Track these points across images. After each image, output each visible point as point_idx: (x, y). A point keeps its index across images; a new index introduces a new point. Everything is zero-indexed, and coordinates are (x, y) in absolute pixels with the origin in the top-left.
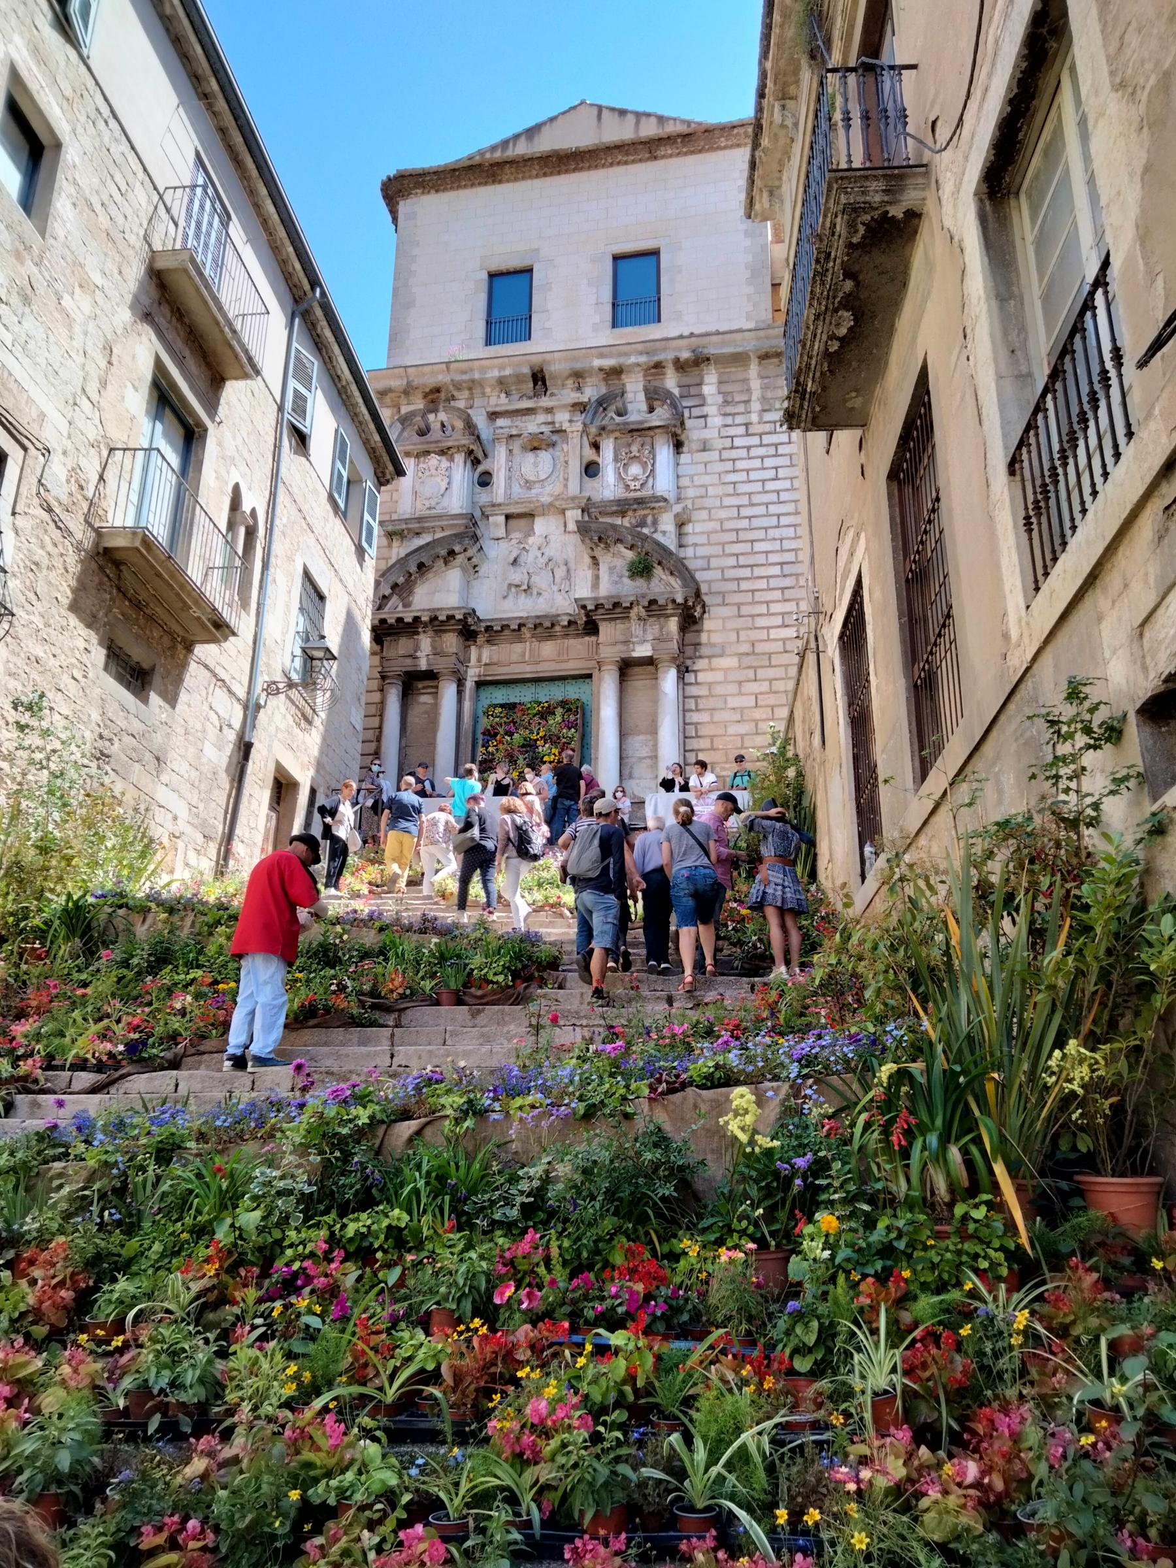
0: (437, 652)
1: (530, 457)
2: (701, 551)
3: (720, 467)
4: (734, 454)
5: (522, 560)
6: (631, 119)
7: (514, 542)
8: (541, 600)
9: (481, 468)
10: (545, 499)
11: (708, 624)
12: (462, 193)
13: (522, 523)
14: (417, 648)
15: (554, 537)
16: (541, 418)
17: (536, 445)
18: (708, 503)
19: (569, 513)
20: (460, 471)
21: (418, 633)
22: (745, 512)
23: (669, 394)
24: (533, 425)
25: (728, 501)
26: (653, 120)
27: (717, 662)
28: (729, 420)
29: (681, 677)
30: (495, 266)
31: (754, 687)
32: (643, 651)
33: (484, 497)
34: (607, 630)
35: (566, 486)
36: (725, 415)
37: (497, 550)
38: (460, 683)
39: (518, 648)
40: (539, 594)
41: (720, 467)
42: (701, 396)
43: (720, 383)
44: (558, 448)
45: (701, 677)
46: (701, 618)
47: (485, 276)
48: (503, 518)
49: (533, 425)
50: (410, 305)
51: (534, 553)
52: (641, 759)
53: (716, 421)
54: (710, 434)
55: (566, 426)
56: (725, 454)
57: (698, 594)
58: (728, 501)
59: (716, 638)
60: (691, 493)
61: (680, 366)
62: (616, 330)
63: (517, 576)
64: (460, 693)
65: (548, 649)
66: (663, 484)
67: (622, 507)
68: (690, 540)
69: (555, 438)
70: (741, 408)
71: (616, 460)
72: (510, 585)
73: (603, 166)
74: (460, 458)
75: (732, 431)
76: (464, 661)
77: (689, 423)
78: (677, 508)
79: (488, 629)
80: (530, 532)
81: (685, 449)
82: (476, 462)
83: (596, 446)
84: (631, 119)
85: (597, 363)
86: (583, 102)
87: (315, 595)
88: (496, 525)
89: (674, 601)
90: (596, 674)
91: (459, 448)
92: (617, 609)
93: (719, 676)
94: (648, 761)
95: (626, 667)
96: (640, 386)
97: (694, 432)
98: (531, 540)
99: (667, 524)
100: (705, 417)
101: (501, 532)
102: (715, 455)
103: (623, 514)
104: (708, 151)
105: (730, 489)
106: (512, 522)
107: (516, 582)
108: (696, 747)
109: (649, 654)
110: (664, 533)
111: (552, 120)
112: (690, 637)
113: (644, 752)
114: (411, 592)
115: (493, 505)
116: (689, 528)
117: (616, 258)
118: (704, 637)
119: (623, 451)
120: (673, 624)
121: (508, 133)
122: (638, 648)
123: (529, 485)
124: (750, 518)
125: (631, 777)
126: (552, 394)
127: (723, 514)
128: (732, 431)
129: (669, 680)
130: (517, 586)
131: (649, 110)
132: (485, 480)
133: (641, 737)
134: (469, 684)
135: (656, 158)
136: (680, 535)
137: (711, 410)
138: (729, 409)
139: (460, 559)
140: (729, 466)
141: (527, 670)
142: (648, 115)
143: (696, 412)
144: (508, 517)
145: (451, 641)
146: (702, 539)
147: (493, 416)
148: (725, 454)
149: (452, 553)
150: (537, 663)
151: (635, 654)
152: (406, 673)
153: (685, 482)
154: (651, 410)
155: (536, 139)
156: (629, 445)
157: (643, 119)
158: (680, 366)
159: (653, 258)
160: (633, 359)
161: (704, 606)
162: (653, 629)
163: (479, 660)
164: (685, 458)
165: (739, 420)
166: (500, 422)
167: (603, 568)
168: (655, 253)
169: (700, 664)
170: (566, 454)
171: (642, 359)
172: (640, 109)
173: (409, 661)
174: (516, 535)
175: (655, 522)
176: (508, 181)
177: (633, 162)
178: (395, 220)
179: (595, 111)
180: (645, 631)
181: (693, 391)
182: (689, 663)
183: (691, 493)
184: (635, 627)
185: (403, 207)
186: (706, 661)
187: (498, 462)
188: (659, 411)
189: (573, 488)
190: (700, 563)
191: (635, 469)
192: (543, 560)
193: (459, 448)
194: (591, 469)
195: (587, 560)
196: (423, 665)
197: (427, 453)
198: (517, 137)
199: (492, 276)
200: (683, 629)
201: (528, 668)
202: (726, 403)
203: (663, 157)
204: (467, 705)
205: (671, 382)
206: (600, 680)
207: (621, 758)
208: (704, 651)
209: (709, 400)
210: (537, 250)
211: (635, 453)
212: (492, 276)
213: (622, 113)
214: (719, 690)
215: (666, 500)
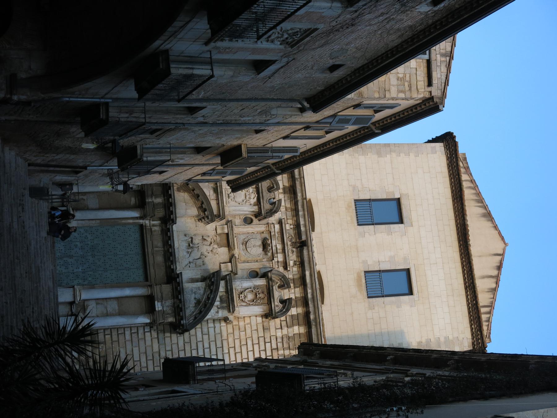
0: (154, 205)
1: (259, 243)
2: (211, 331)
3: (255, 336)
4: (262, 343)
5: (205, 243)
6: (495, 273)
7: (215, 238)
8: (185, 253)
9: (253, 218)
10: (236, 252)
11: (174, 336)
12: (447, 179)
13: (225, 241)
14: (156, 197)
15: (216, 258)
16: (279, 247)
17: (265, 245)
18: (237, 333)
19: (230, 264)
20: (249, 209)
21: (164, 197)
22: (232, 350)
23: (288, 310)
24: (276, 244)
25: (237, 342)
26: (494, 286)
27: (155, 341)
28: (279, 340)
29: (147, 324)
30: (403, 202)
31: (143, 360)
32: (158, 306)
33: (237, 221)
34: (167, 289)
35: (244, 262)
36: (282, 338)
37: (210, 229)
38: (141, 218)
39: (160, 244)
40: (188, 252)
41: (255, 336)
42: (293, 325)
43: (300, 334)
44: (264, 256)
45: (148, 335)
46: (177, 333)
47: (397, 196)
48: (226, 231)
49: (276, 244)
50: (379, 154)
51: (210, 248)
52: (106, 308)
53: (279, 334)
54: (273, 332)
55: (276, 259)
56: (262, 340)
57: (187, 330)
58: (237, 342)
59: (168, 340)
60: (242, 324)
61: (307, 314)
62: (363, 274)
63: (197, 240)
64: (137, 218)
65: (160, 259)
66: (242, 311)
67: (229, 291)
68: (217, 325)
69: (270, 254)
70: (286, 345)
71: (255, 287)
72: (192, 238)
73: (461, 259)
74: (255, 209)
75: (274, 342)
76: (152, 217)
77: (278, 321)
78: (231, 317)
79: (168, 230)
80: (220, 246)
81: (264, 319)
82: (256, 216)
83: (264, 275)
84: (495, 273)
85: (307, 273)
86: (506, 244)
87: (161, 173)
88: (223, 229)
89: (182, 319)
90: (148, 283)
91: (260, 208)
92: (177, 292)
93: (149, 343)
94: (105, 312)
95: (150, 300)
96: (293, 296)
97: (274, 323)
98: (216, 246)
99: (222, 313)
100: (281, 328)
101: (219, 231)
102: (261, 334)
103: (227, 291)
104: (470, 318)
105: (243, 342)
107: (194, 241)
108: (113, 334)
109: (157, 309)
110: (218, 312)
111: (496, 227)
112: (168, 327)
113: (110, 310)
114: (185, 191)
116: (223, 324)
117: (408, 271)
118: (168, 335)
119: (260, 291)
120: (171, 319)
121: (488, 201)
122: (159, 304)
123: (245, 243)
124: (229, 352)
125: (97, 304)
126: (293, 252)
127: (231, 340)
128: (274, 342)
129: (144, 320)
130: (192, 241)
131: (501, 283)
132: (248, 221)
133: (117, 308)
134: (141, 221)
135: (466, 288)
136: (220, 320)
137: (285, 331)
138: (285, 339)
139: (202, 214)
140: (256, 341)
141: (149, 250)
142: (497, 283)
143: (284, 323)
144: (227, 234)
145: (160, 213)
146: (218, 330)
147: (280, 222)
148: (262, 340)
149: (205, 210)
150: (153, 254)
151: (156, 302)
152: (144, 192)
153: (247, 320)
154: (283, 302)
155: (483, 219)
156: (263, 293)
157: (494, 280)
158: (307, 314)
159: (407, 291)
160: (309, 291)
161: (182, 333)
162: (168, 309)
163: (154, 225)
164: (259, 319)
165: (280, 345)
166: (277, 227)
167: (199, 284)
168: (411, 293)
169: (154, 334)
170: (261, 261)
171: (310, 296)
172: (502, 277)
173: (150, 193)
174: (218, 239)
175: (222, 308)
176: (454, 205)
177: (464, 276)
178: (429, 142)
179: (501, 252)
180: (168, 306)
181: (295, 322)
182: (155, 328)
183: (242, 324)
184: (169, 303)
185: (440, 146)
186: (156, 336)
187: (258, 227)
188: (281, 306)
189: (240, 266)
190: (205, 330)
191: (250, 297)
192: (206, 253)
193: (260, 208)
194: (254, 275)
195: (206, 275)
196: (149, 200)
197: (258, 193)
198: (485, 207)
199: (398, 200)
200: (171, 324)
201: (150, 250)
202: (289, 338)
203: (466, 292)
204: (131, 221)
205: (294, 311)
206: (143, 286)
207: (106, 299)
208: (161, 336)
209: (290, 330)
210: (412, 226)
211: (258, 296)
212: (398, 200)
213: (499, 268)
214: (142, 343)
215: (233, 312)
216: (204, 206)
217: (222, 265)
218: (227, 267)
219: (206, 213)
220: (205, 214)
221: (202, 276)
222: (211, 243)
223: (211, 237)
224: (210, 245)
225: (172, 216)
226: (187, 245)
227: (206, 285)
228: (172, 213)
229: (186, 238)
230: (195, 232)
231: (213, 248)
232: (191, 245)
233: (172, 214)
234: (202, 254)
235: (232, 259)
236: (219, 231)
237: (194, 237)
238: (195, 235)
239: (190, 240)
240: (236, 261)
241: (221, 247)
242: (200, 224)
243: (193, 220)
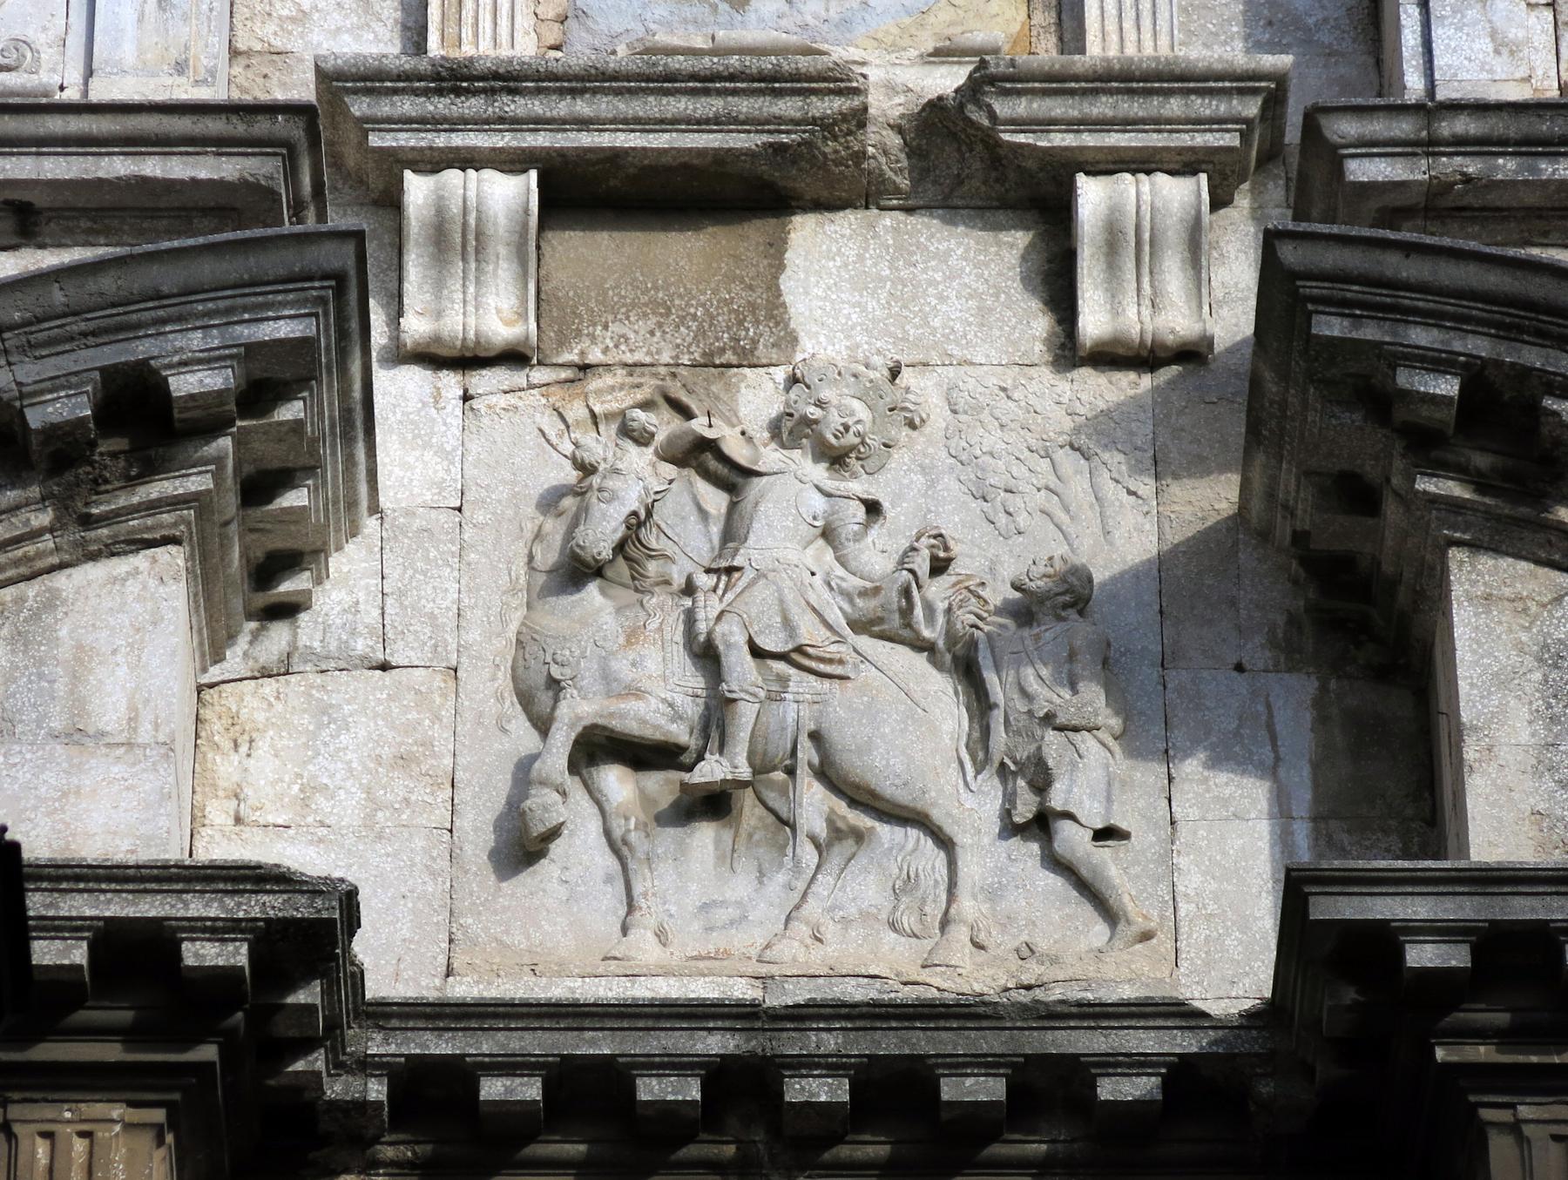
7: (609, 394)
8: (862, 886)
13: (681, 253)
72: (599, 747)
80: (751, 329)
88: (458, 241)
98: (757, 397)
106: (592, 253)
115: (455, 79)
216: (69, 407)
217: (1094, 323)
218: (1131, 244)
219: (183, 384)
220: (207, 420)
221: (1289, 654)
222: (698, 455)
223: (599, 446)
224: (734, 478)
225: (200, 953)
226: (705, 835)
227: (1499, 537)
228: (135, 957)
229: (581, 850)
230: (489, 687)
231: (790, 429)
232: (712, 770)
233: (158, 941)
234: (888, 619)
235: (991, 166)
236: (495, 310)
237: (579, 709)
238: (537, 698)
239: (616, 781)
240: (1056, 83)
241: (774, 310)
242: (346, 589)
243: (253, 702)
